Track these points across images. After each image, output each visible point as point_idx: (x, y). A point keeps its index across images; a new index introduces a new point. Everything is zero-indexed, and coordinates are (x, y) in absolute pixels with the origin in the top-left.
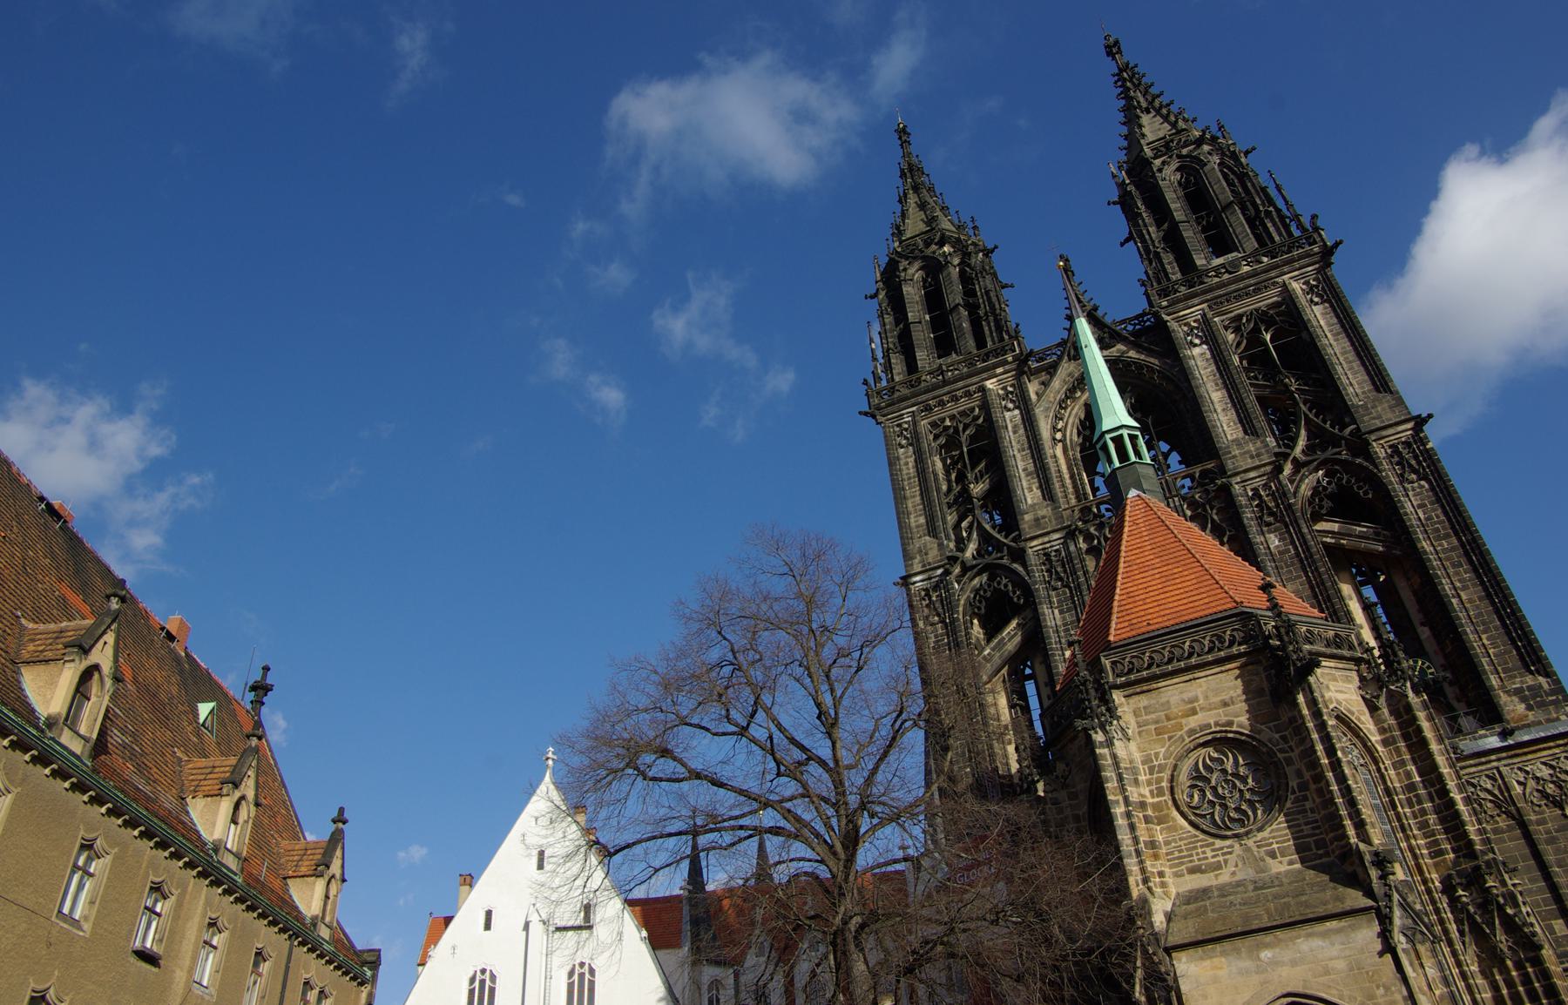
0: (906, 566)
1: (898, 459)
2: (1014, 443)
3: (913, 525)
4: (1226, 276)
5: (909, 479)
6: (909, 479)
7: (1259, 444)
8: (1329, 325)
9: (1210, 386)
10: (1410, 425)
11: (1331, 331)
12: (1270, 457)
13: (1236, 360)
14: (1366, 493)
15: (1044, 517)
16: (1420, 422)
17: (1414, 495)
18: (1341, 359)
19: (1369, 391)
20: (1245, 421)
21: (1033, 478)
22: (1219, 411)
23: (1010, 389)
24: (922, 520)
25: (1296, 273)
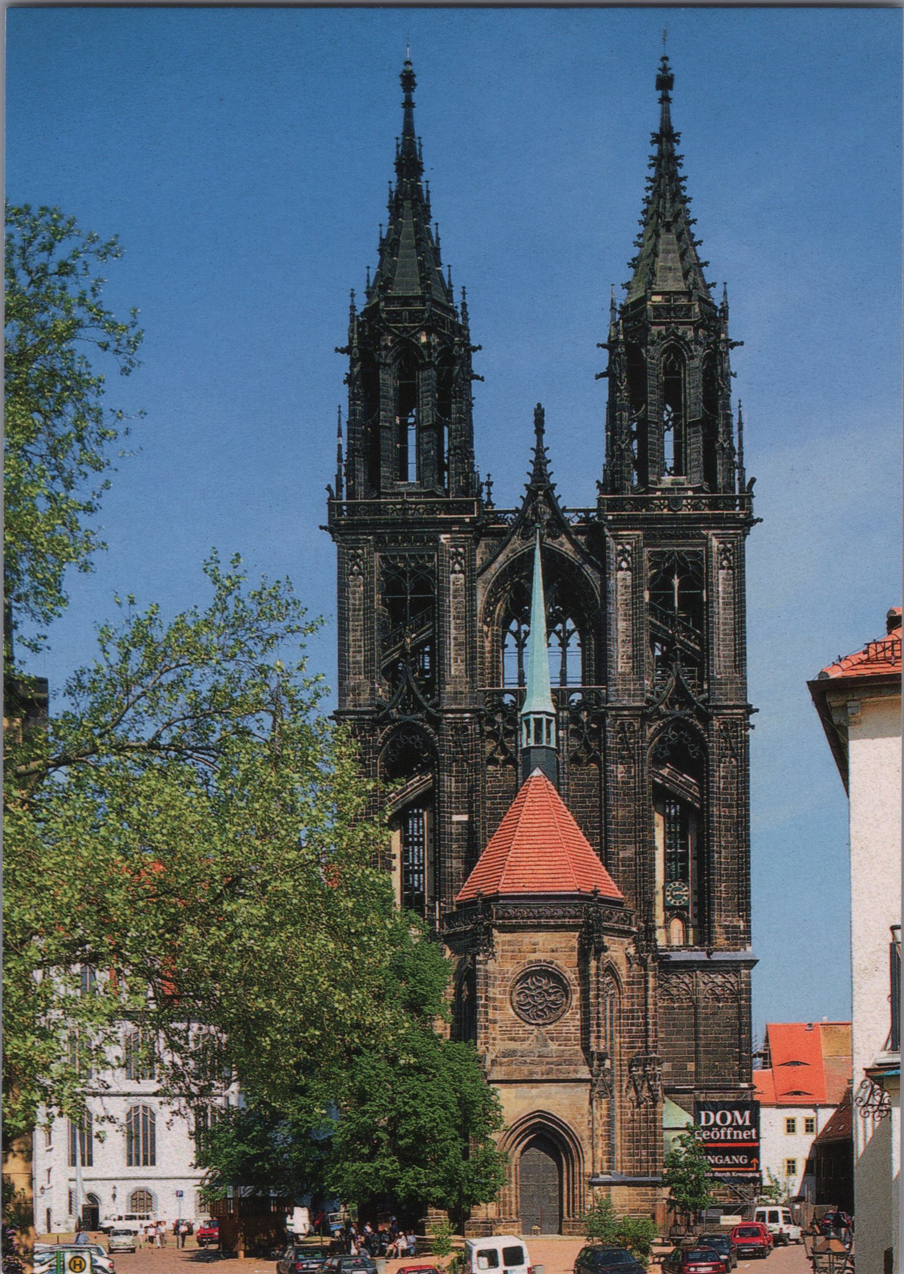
0: (340, 700)
1: (349, 586)
2: (452, 610)
3: (351, 659)
4: (665, 511)
5: (354, 610)
6: (354, 610)
7: (637, 686)
8: (724, 592)
9: (621, 612)
10: (741, 711)
11: (723, 598)
12: (641, 701)
13: (647, 595)
14: (694, 754)
15: (461, 693)
16: (750, 710)
17: (724, 767)
18: (722, 628)
19: (730, 667)
20: (636, 658)
21: (460, 650)
22: (619, 641)
23: (461, 550)
24: (360, 658)
25: (719, 532)
